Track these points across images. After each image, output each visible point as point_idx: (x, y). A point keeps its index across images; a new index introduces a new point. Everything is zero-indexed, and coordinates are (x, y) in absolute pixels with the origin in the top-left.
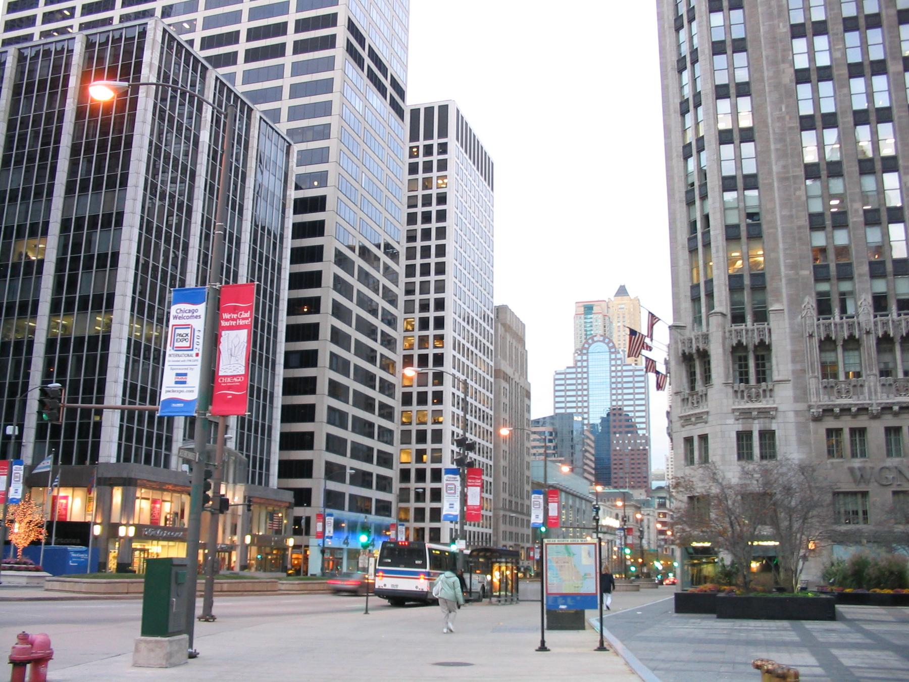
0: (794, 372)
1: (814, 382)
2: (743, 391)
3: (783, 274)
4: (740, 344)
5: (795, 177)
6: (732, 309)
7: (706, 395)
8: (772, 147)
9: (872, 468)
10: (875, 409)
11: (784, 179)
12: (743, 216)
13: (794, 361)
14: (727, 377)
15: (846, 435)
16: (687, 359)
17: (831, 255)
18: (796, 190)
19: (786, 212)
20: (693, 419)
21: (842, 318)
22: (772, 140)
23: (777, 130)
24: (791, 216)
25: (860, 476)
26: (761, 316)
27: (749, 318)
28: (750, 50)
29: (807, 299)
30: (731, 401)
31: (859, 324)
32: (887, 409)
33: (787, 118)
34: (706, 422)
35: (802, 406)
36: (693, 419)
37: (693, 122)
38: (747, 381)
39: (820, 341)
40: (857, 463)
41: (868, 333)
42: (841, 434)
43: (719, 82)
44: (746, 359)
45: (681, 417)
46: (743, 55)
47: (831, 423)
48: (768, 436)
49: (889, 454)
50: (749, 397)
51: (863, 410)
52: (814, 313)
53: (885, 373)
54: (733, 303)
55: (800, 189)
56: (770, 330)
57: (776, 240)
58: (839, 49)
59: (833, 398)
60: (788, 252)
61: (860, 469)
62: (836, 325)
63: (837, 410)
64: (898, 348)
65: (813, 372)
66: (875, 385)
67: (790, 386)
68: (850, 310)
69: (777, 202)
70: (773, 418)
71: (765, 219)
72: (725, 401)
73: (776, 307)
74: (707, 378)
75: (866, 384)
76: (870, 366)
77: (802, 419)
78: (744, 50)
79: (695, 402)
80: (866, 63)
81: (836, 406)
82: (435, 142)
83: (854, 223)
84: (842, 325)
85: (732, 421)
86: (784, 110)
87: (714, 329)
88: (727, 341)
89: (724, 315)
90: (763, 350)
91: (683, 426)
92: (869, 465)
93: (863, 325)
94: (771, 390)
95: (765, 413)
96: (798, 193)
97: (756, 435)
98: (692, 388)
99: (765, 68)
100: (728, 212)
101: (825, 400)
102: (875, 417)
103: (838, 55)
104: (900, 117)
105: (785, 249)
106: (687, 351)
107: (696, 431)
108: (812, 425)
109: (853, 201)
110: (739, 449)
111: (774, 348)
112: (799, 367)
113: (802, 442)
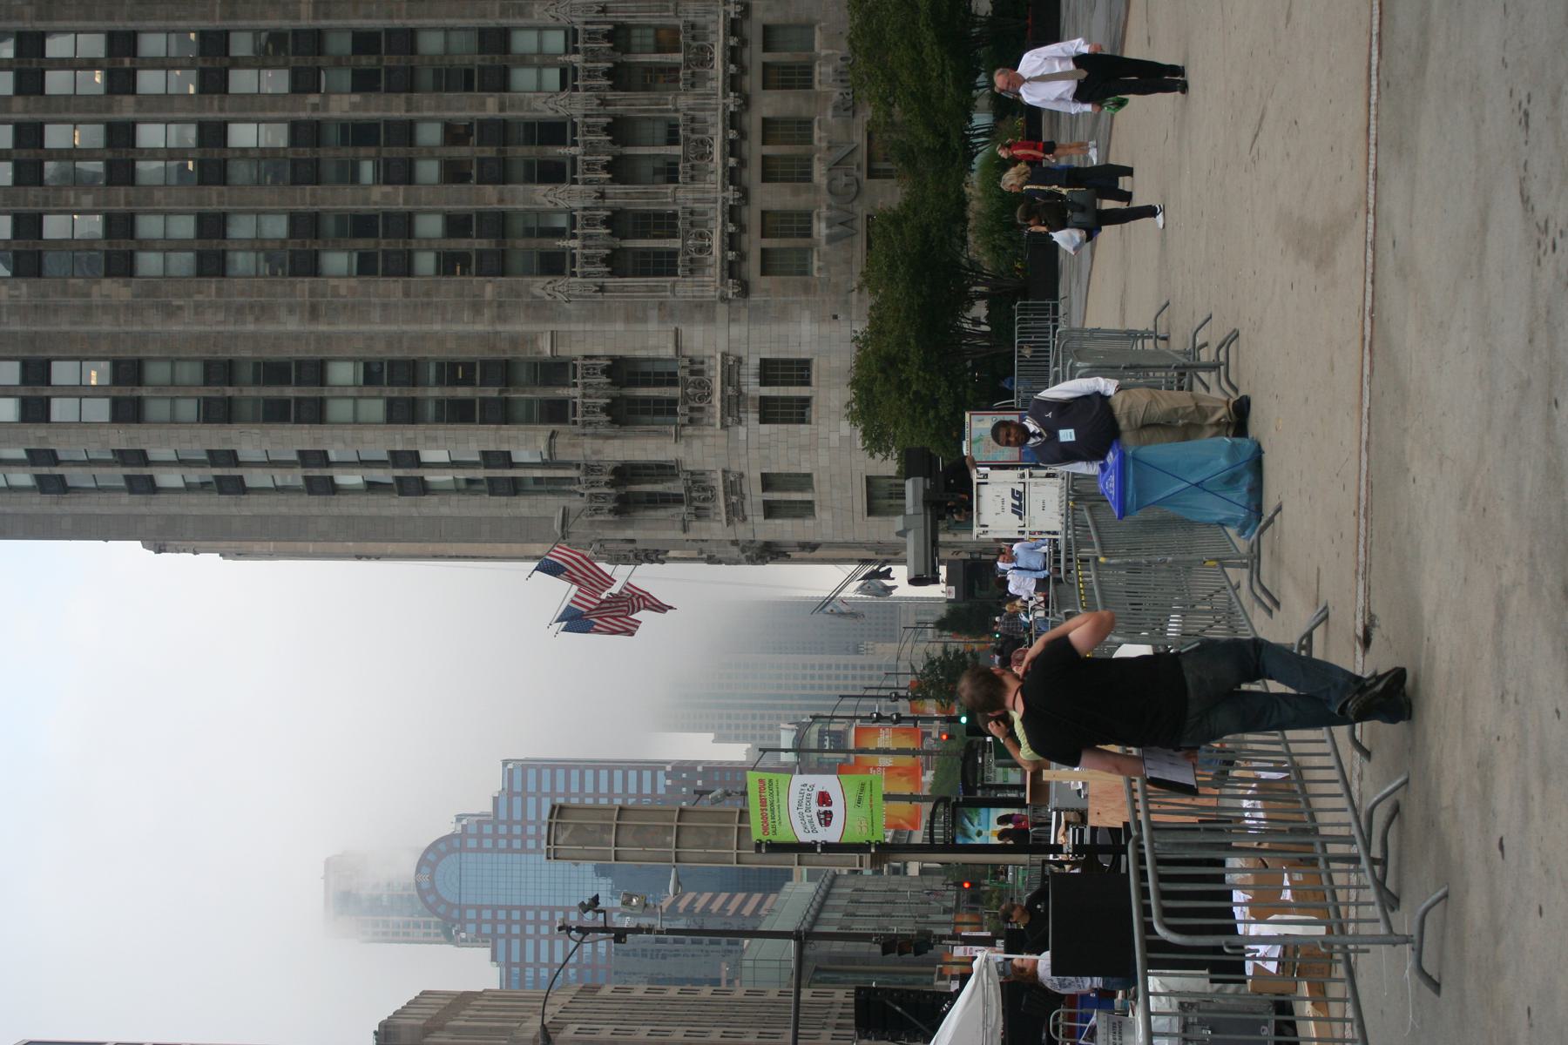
0: (662, 321)
1: (684, 288)
2: (692, 409)
3: (489, 329)
4: (607, 409)
5: (312, 293)
6: (541, 422)
7: (692, 473)
8: (250, 327)
9: (829, 207)
10: (732, 194)
11: (314, 313)
12: (374, 391)
13: (645, 320)
14: (667, 434)
15: (770, 243)
16: (626, 506)
17: (462, 244)
18: (338, 295)
19: (376, 314)
20: (734, 499)
21: (574, 236)
22: (238, 328)
23: (221, 317)
24: (385, 306)
25: (843, 225)
26: (555, 370)
27: (562, 392)
28: (52, 354)
29: (537, 291)
30: (709, 431)
31: (585, 209)
32: (732, 176)
33: (199, 297)
34: (742, 475)
35: (722, 309)
36: (734, 499)
37: (175, 470)
38: (673, 402)
39: (612, 274)
40: (820, 229)
42: (769, 255)
44: (634, 401)
45: (729, 522)
46: (56, 367)
47: (753, 266)
48: (771, 371)
49: (806, 176)
50: (701, 399)
51: (733, 214)
52: (561, 281)
53: (669, 173)
54: (529, 420)
55: (335, 288)
56: (586, 357)
57: (423, 337)
58: (77, 197)
59: (711, 260)
60: (449, 316)
61: (829, 226)
62: (584, 247)
63: (731, 255)
64: (630, 151)
65: (664, 289)
66: (693, 191)
67: (684, 329)
68: (562, 222)
69: (353, 328)
70: (739, 360)
71: (381, 351)
72: (709, 441)
74: (664, 470)
75: (689, 204)
76: (656, 195)
77: (744, 313)
78: (47, 364)
79: (703, 495)
80: (109, 155)
81: (723, 258)
83: (406, 202)
84: (586, 237)
85: (742, 430)
86: (177, 302)
87: (580, 451)
88: (602, 430)
89: (553, 435)
90: (621, 370)
91: (745, 519)
92: (824, 211)
93: (588, 203)
94: (692, 361)
96: (343, 291)
97: (767, 391)
98: (676, 500)
99: (97, 328)
100: (362, 417)
103: (87, 201)
104: (221, 110)
105: (444, 320)
106: (611, 506)
107: (755, 495)
108: (755, 298)
109: (366, 201)
110: (790, 422)
111: (619, 352)
112: (654, 313)
113: (783, 315)
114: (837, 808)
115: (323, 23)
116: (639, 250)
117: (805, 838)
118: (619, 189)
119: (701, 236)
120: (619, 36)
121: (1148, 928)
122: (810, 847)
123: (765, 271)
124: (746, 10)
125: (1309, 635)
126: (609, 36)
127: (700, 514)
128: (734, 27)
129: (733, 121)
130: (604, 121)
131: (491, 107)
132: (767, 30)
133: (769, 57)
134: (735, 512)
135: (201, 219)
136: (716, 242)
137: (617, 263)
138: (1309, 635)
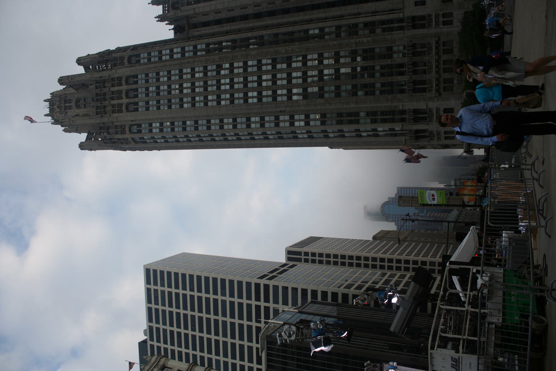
4: (413, 119)
10: (437, 76)
16: (417, 138)
17: (384, 89)
26: (403, 112)
27: (404, 116)
32: (437, 72)
38: (426, 117)
40: (455, 82)
41: (411, 78)
43: (320, 124)
47: (442, 90)
51: (437, 80)
53: (424, 72)
68: (403, 83)
73: (401, 108)
74: (425, 131)
82: (303, 257)
90: (416, 111)
95: (438, 110)
101: (434, 92)
102: (440, 76)
103: (315, 85)
107: (443, 135)
114: (436, 197)
115: (357, 48)
116: (419, 88)
117: (430, 203)
118: (414, 76)
119: (431, 84)
120: (414, 46)
121: (487, 222)
122: (431, 205)
123: (444, 91)
124: (439, 39)
125: (534, 162)
126: (412, 46)
127: (432, 139)
128: (437, 42)
129: (437, 61)
130: (411, 63)
131: (389, 62)
132: (444, 42)
133: (444, 48)
134: (439, 139)
135: (336, 87)
136: (434, 86)
137: (414, 91)
138: (534, 162)
